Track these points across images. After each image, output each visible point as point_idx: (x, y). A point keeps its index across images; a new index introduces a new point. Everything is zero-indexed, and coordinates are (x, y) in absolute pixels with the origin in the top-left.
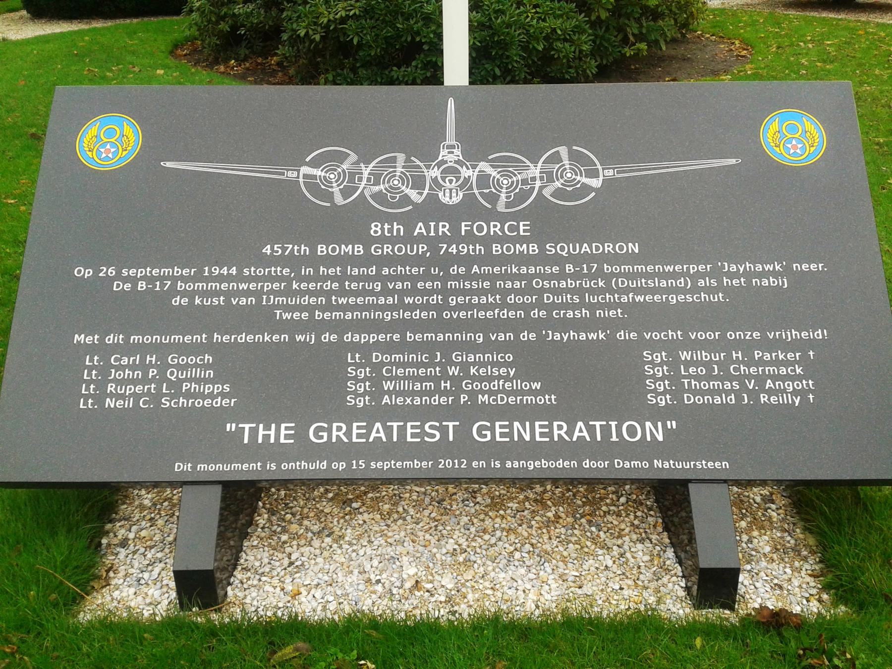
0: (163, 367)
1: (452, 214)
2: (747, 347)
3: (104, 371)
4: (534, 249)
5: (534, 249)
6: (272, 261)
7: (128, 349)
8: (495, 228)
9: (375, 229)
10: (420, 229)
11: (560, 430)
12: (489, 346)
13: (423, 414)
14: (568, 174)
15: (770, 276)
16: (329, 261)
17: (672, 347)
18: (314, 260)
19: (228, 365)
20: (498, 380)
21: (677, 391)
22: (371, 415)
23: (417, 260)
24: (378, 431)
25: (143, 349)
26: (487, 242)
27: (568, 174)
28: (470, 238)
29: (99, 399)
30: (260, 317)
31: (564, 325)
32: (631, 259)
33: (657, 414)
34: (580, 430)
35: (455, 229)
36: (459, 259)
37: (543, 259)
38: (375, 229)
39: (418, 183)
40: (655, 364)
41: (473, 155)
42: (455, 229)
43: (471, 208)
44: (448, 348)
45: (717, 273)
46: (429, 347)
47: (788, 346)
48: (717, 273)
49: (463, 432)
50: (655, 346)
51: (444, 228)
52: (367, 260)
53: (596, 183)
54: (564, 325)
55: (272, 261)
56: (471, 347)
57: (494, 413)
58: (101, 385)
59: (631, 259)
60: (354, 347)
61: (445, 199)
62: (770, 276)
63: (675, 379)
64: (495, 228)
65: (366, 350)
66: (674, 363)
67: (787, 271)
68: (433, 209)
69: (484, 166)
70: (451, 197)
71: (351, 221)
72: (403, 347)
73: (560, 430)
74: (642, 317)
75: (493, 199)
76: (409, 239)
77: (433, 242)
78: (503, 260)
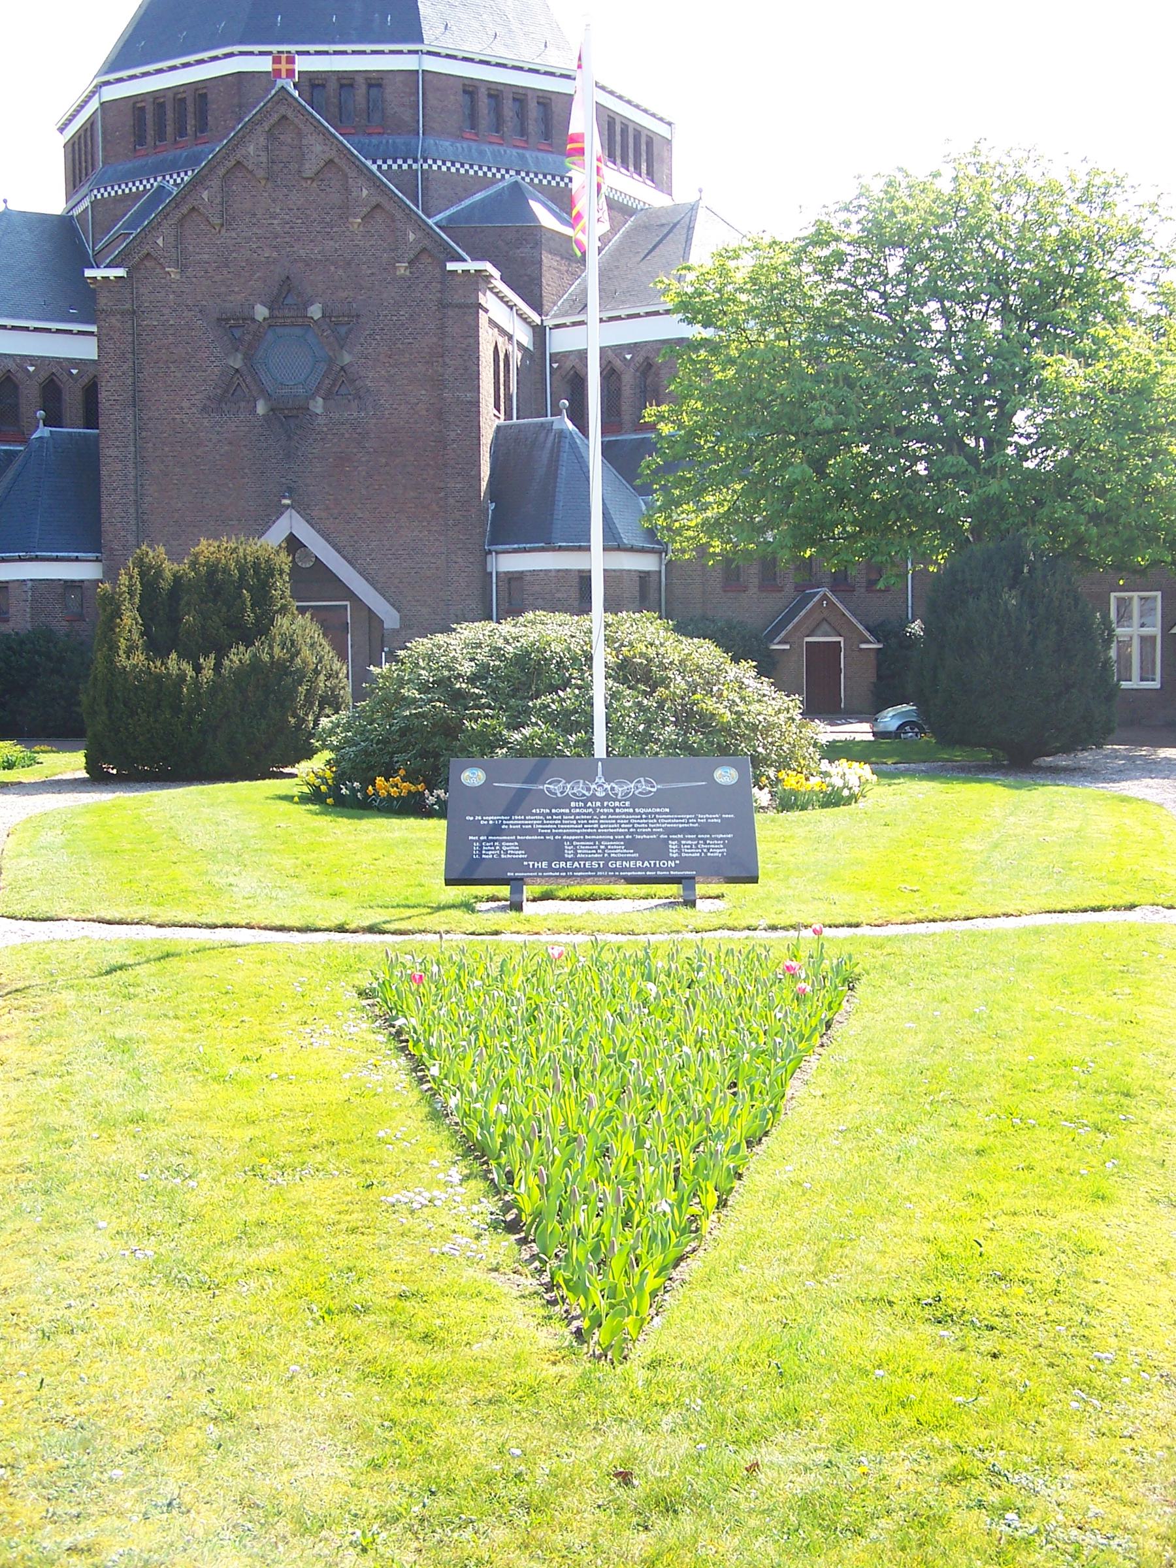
0: (501, 846)
1: (602, 800)
2: (705, 840)
3: (481, 847)
4: (631, 810)
5: (631, 810)
6: (536, 814)
7: (488, 841)
8: (617, 804)
9: (573, 804)
10: (589, 804)
11: (639, 864)
12: (614, 840)
13: (592, 860)
14: (644, 787)
15: (715, 819)
16: (556, 814)
17: (679, 840)
18: (551, 814)
19: (522, 845)
20: (619, 850)
21: (680, 852)
22: (573, 860)
23: (589, 814)
24: (576, 864)
25: (494, 841)
26: (614, 808)
27: (644, 787)
28: (608, 807)
29: (480, 855)
30: (533, 831)
31: (642, 834)
32: (666, 813)
33: (672, 859)
34: (646, 864)
35: (602, 804)
36: (604, 814)
37: (634, 813)
38: (573, 804)
39: (588, 789)
40: (673, 845)
41: (608, 780)
42: (602, 804)
43: (607, 797)
44: (600, 841)
45: (696, 818)
46: (594, 840)
47: (717, 839)
48: (696, 818)
49: (606, 865)
50: (673, 840)
51: (598, 804)
52: (570, 814)
53: (654, 790)
54: (642, 834)
55: (536, 814)
56: (610, 840)
57: (616, 859)
58: (481, 851)
59: (666, 813)
60: (567, 840)
61: (598, 794)
62: (715, 819)
63: (680, 849)
64: (617, 804)
65: (571, 841)
66: (680, 845)
67: (720, 818)
68: (593, 798)
69: (613, 784)
70: (600, 794)
71: (565, 802)
72: (584, 840)
73: (639, 864)
74: (669, 831)
75: (616, 795)
76: (585, 807)
77: (594, 809)
78: (620, 814)
